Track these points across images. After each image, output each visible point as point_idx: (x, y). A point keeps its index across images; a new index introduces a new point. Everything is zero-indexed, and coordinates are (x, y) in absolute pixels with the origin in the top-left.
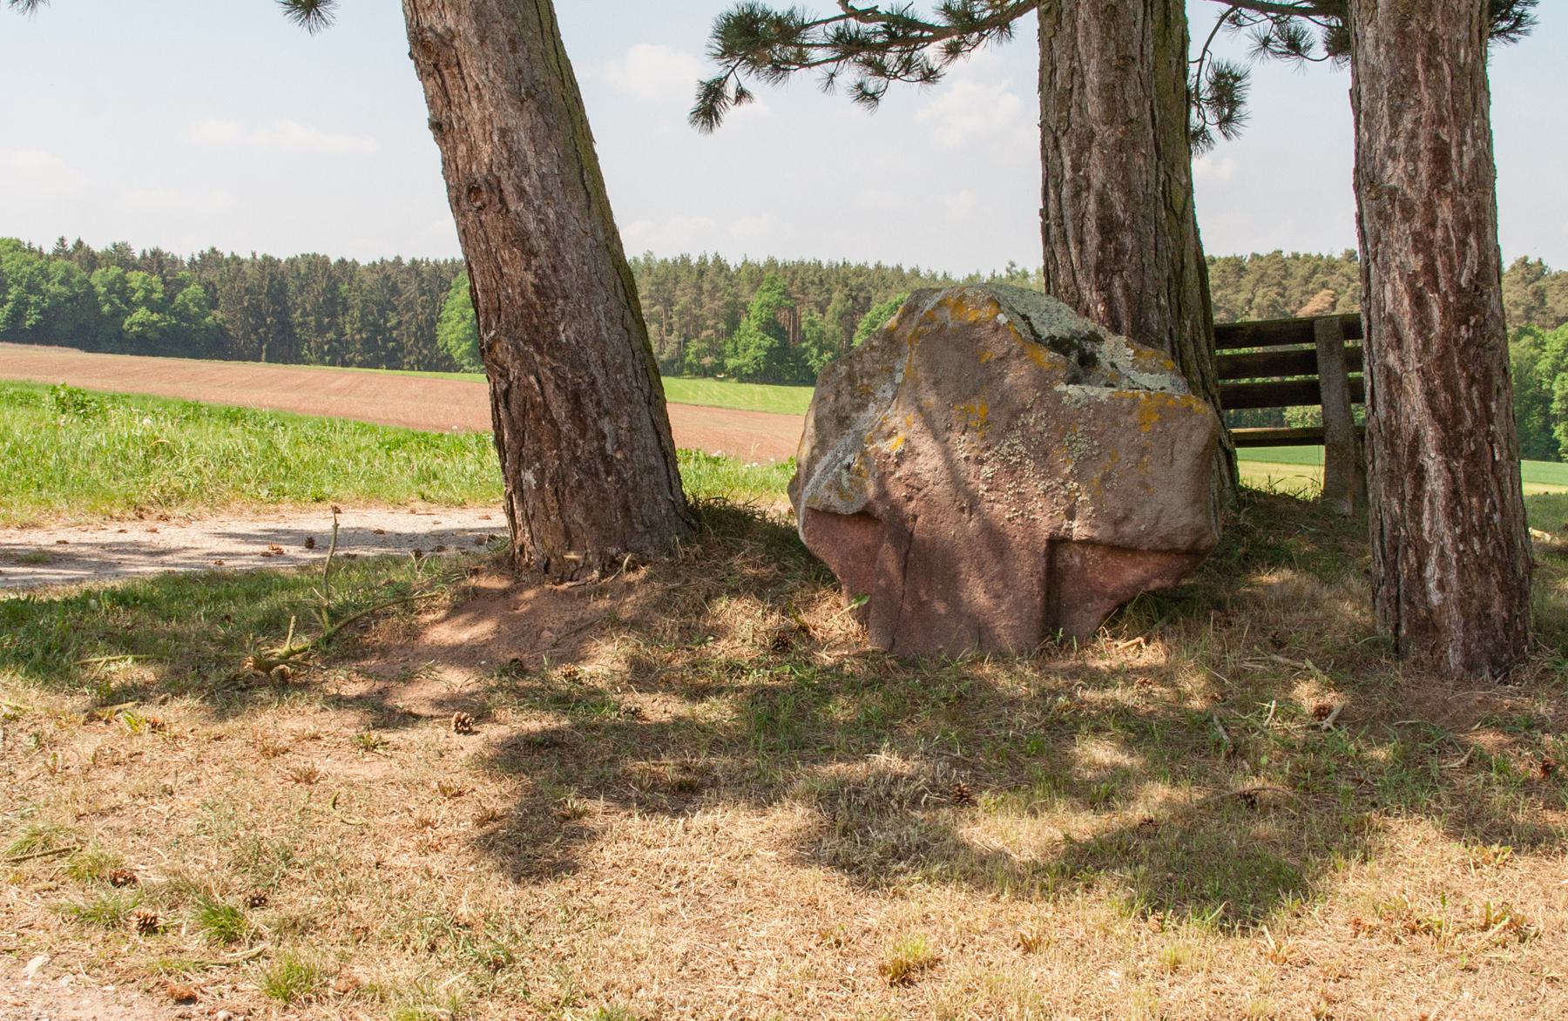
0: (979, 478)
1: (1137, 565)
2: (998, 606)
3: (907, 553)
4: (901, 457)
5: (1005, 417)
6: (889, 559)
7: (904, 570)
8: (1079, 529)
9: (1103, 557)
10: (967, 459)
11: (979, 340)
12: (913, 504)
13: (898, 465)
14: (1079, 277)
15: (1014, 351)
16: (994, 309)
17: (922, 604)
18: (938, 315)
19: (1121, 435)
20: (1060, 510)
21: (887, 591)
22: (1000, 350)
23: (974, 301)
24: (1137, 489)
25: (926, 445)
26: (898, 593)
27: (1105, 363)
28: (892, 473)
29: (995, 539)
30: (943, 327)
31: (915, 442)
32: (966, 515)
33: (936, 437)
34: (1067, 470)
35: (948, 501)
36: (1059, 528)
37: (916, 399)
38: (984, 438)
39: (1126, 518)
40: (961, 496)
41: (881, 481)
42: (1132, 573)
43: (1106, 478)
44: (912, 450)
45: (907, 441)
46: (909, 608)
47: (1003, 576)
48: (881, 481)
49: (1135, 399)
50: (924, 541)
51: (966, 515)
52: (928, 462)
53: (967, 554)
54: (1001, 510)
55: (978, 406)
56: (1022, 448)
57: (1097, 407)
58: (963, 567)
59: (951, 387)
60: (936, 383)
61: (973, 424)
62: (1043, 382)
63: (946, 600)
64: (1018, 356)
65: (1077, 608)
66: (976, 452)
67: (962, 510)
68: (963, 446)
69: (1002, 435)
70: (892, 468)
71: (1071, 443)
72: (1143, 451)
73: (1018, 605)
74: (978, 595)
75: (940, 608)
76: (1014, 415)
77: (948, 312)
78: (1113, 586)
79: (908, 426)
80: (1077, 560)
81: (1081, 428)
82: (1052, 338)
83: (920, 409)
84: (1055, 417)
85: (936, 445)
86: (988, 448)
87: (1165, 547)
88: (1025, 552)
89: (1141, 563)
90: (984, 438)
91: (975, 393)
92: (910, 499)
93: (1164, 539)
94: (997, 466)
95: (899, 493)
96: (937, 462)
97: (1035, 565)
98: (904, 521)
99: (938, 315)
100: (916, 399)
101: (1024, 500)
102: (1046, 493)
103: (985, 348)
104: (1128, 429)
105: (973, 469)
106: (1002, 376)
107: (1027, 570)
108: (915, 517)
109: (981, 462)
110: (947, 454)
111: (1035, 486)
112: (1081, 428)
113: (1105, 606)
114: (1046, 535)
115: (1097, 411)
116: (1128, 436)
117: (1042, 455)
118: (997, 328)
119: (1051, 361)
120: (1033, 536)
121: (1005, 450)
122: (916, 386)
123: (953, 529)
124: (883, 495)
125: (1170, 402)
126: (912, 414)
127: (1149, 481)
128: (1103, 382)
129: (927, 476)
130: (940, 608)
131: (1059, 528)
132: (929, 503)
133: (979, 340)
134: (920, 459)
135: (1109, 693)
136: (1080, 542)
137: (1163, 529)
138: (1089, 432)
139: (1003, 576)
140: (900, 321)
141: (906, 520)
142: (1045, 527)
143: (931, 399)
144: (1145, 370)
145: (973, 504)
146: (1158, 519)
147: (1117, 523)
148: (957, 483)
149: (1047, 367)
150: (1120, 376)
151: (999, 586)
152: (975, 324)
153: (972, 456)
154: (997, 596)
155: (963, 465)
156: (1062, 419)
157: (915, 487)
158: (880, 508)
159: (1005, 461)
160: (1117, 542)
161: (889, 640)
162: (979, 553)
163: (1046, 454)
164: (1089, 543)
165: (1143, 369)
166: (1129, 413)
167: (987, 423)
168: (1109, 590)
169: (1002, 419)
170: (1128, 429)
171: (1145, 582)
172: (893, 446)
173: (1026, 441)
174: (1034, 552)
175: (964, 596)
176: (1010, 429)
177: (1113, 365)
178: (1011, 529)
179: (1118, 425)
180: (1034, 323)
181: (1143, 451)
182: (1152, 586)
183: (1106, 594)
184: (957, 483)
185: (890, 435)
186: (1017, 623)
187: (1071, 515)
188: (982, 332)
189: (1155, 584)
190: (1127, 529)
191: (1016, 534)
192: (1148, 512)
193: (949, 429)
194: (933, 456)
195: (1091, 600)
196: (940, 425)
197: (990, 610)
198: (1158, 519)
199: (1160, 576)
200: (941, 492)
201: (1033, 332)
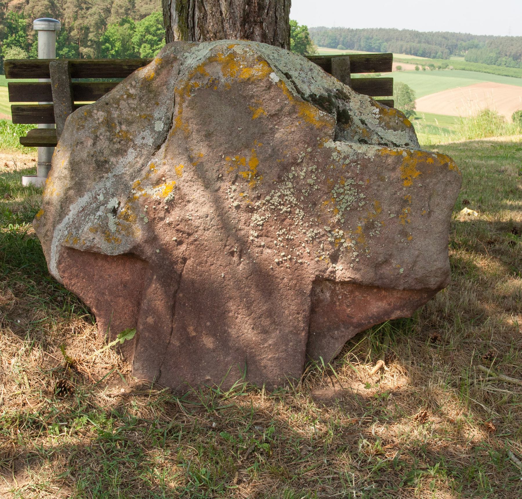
0: (249, 227)
1: (381, 300)
2: (265, 340)
3: (176, 292)
4: (171, 204)
5: (276, 170)
6: (156, 296)
7: (173, 309)
8: (342, 271)
9: (351, 292)
10: (238, 207)
11: (252, 97)
12: (183, 247)
13: (168, 211)
14: (227, 26)
15: (287, 109)
16: (266, 68)
17: (190, 340)
18: (208, 70)
19: (385, 189)
20: (325, 255)
21: (155, 328)
22: (273, 108)
23: (245, 59)
24: (398, 237)
25: (197, 193)
26: (166, 329)
27: (356, 120)
28: (162, 219)
29: (263, 280)
30: (214, 83)
31: (185, 190)
32: (235, 258)
33: (207, 185)
34: (335, 220)
35: (219, 246)
36: (324, 271)
37: (187, 150)
38: (254, 188)
39: (386, 262)
40: (231, 241)
41: (150, 226)
42: (376, 306)
43: (369, 227)
44: (182, 198)
45: (177, 188)
46: (178, 344)
47: (270, 314)
48: (150, 226)
49: (399, 156)
50: (193, 282)
51: (235, 258)
52: (198, 207)
53: (235, 293)
54: (271, 255)
55: (249, 159)
56: (293, 199)
57: (364, 163)
58: (232, 306)
59: (223, 139)
60: (208, 136)
61: (244, 175)
62: (313, 138)
63: (214, 335)
64: (290, 114)
65: (325, 336)
66: (247, 201)
67: (232, 254)
68: (233, 195)
69: (272, 187)
70: (162, 214)
71: (339, 194)
72: (405, 202)
73: (284, 339)
74: (244, 328)
75: (208, 342)
76: (285, 168)
77: (219, 67)
78: (359, 316)
79: (178, 175)
80: (328, 295)
81: (350, 181)
82: (313, 96)
83: (191, 159)
84: (324, 171)
85: (207, 194)
86: (259, 198)
87: (418, 287)
88: (292, 292)
89: (385, 297)
90: (254, 188)
91: (247, 146)
92: (180, 243)
93: (418, 281)
94: (268, 215)
95: (168, 237)
96: (207, 209)
97: (302, 304)
98: (174, 263)
99: (208, 70)
100: (187, 150)
101: (293, 246)
102: (313, 239)
103: (257, 105)
104: (391, 183)
105: (244, 216)
106: (273, 131)
107: (292, 310)
108: (185, 260)
109: (251, 210)
110: (217, 202)
111: (303, 232)
112: (350, 181)
113: (350, 333)
114: (312, 277)
115: (364, 167)
116: (391, 190)
117: (310, 203)
118: (270, 86)
119: (321, 119)
120: (300, 278)
121: (276, 200)
122: (186, 138)
123: (223, 269)
124: (153, 239)
125: (430, 160)
126: (181, 164)
127: (409, 230)
128: (356, 138)
129: (197, 223)
130: (208, 342)
131: (324, 271)
132: (199, 247)
133: (252, 97)
134: (190, 206)
135: (397, 428)
136: (343, 283)
137: (420, 272)
138: (358, 186)
139: (270, 314)
140: (158, 71)
141: (176, 263)
142: (310, 271)
143: (201, 150)
144: (389, 128)
145: (244, 248)
146: (415, 263)
147: (377, 266)
148: (226, 226)
149: (318, 125)
150: (371, 132)
151: (266, 322)
152: (248, 82)
153: (243, 204)
154: (265, 331)
155: (233, 213)
156: (331, 174)
157: (185, 231)
158: (148, 251)
159: (275, 210)
160: (377, 283)
161: (156, 373)
162: (248, 294)
163: (315, 204)
164: (353, 284)
165: (388, 126)
166: (394, 169)
167: (257, 175)
168: (355, 320)
169: (275, 169)
170: (391, 183)
171: (387, 313)
172: (162, 193)
173: (297, 192)
174: (301, 292)
175: (233, 332)
176: (280, 180)
177: (363, 122)
178: (279, 272)
179: (383, 180)
180: (296, 81)
181: (405, 202)
182: (393, 317)
183: (352, 324)
184: (226, 226)
185: (159, 182)
186: (283, 355)
187: (334, 258)
188: (253, 90)
189: (396, 314)
190: (386, 270)
191: (284, 277)
192: (407, 257)
193: (220, 179)
194: (203, 204)
195: (338, 328)
196: (212, 174)
197: (257, 344)
198: (415, 263)
199: (401, 308)
200: (209, 236)
201: (298, 91)
